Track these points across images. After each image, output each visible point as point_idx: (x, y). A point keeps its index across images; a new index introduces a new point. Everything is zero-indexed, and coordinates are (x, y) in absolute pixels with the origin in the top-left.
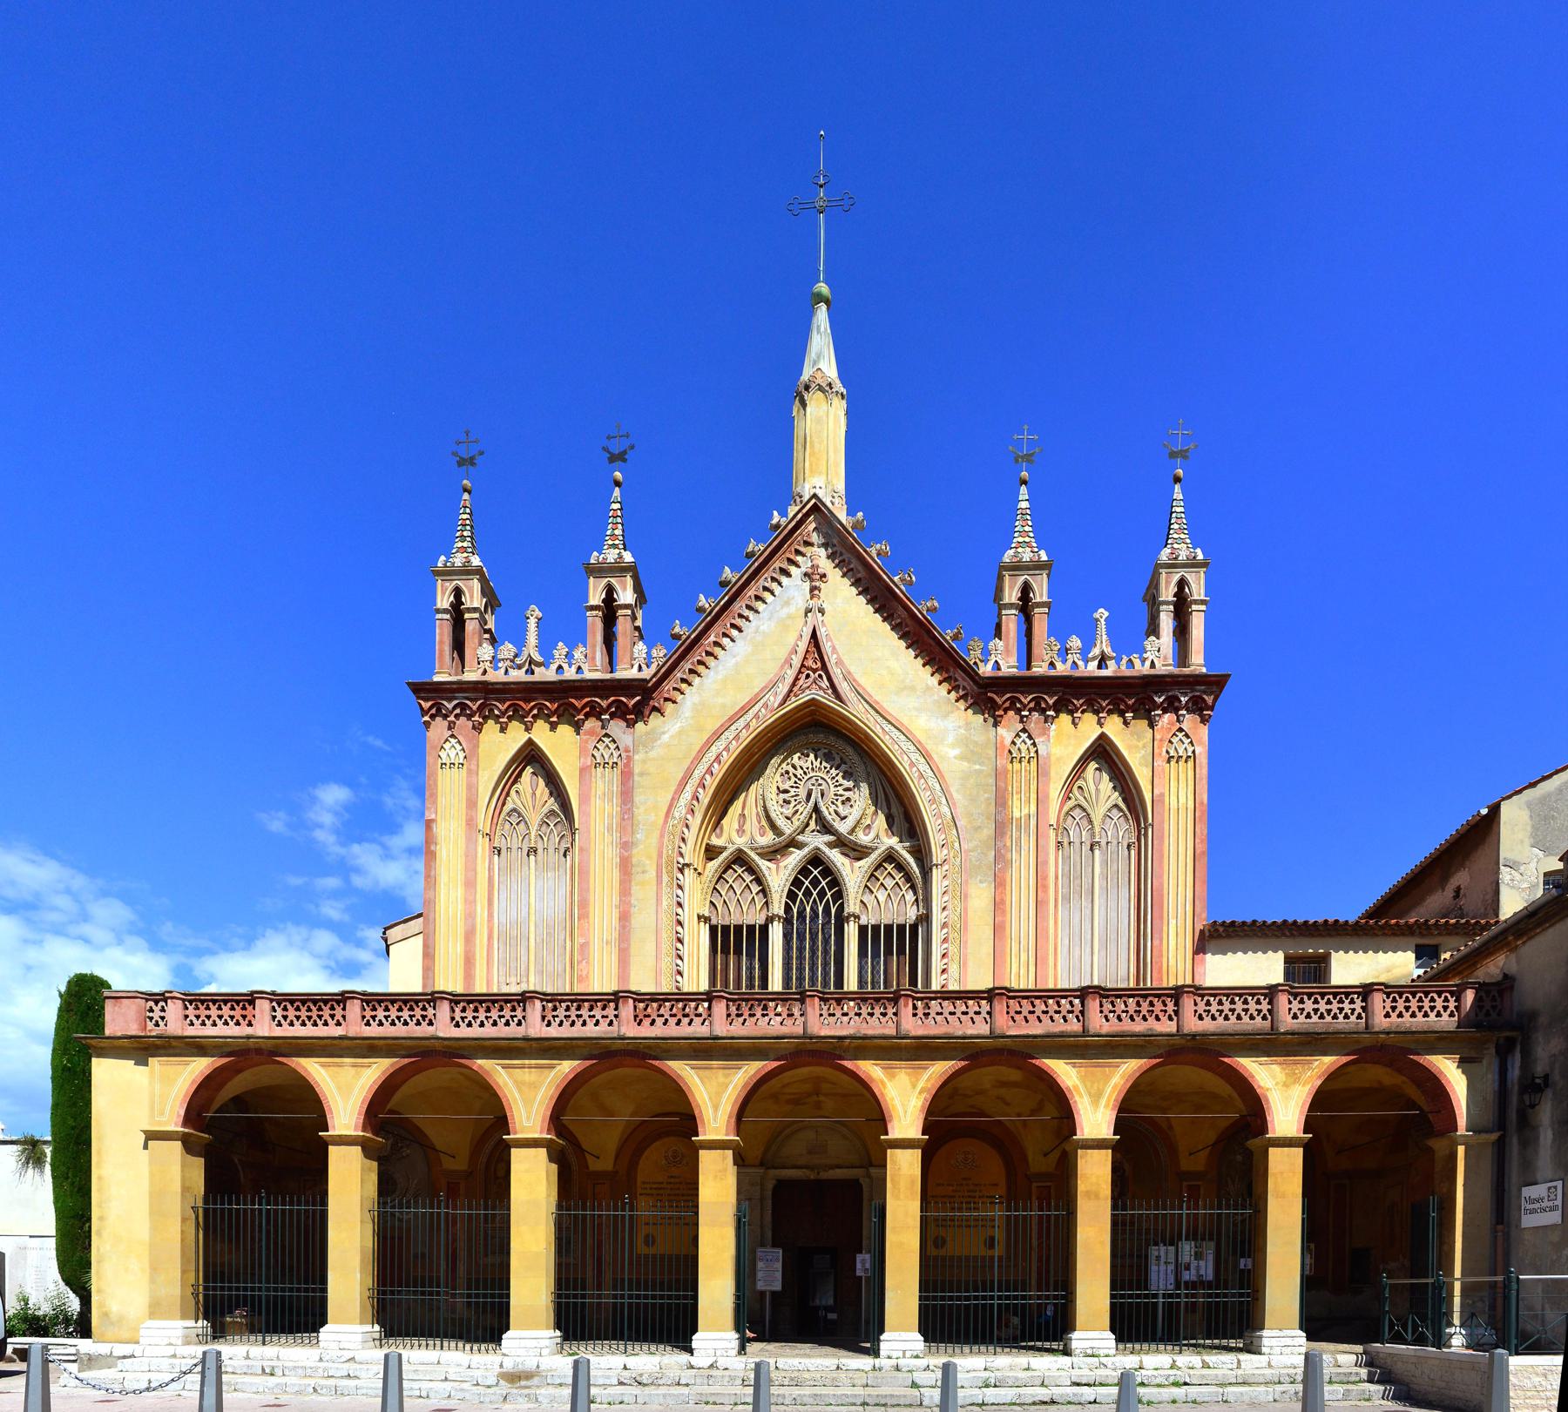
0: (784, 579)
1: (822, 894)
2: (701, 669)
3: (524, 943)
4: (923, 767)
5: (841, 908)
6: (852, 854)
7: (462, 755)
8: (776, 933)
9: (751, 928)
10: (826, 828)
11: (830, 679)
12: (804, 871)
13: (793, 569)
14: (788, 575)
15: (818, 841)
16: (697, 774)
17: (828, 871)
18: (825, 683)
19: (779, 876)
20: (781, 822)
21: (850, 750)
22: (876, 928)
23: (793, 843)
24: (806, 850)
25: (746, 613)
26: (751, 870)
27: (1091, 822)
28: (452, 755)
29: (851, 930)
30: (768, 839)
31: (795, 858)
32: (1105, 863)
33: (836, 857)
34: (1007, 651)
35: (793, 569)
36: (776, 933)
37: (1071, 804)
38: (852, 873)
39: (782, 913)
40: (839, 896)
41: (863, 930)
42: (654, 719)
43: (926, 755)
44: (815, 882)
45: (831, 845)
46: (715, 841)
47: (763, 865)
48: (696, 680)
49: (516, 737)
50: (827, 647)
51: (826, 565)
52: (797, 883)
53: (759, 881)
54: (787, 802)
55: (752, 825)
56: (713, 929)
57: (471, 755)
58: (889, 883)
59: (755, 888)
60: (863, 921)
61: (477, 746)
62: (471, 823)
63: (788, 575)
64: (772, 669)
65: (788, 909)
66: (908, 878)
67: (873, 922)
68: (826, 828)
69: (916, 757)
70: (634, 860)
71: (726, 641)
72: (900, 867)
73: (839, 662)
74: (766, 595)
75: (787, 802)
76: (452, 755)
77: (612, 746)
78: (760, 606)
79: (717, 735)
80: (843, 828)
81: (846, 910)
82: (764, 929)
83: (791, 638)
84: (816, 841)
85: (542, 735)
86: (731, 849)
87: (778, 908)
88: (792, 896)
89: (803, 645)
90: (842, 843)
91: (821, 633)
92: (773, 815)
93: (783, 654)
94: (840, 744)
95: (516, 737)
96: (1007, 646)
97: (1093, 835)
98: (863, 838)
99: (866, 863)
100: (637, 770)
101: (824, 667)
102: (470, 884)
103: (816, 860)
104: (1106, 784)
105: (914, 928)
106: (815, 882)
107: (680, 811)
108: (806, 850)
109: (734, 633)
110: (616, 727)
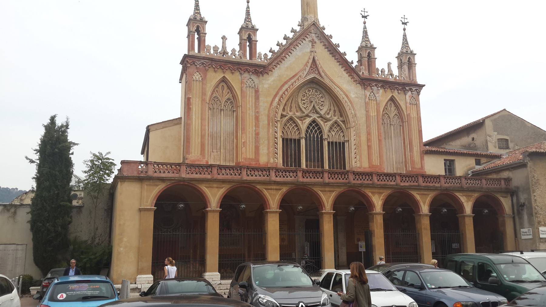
0: (304, 41)
1: (316, 131)
2: (280, 63)
3: (219, 139)
4: (346, 99)
5: (322, 136)
6: (325, 120)
7: (201, 78)
8: (303, 142)
9: (295, 140)
10: (317, 112)
11: (318, 71)
12: (310, 124)
13: (306, 39)
14: (305, 40)
15: (315, 116)
16: (281, 93)
17: (317, 125)
18: (317, 72)
19: (304, 125)
20: (303, 109)
21: (323, 91)
22: (332, 143)
23: (307, 116)
24: (311, 118)
25: (293, 49)
26: (294, 122)
27: (390, 118)
28: (197, 78)
29: (325, 143)
30: (299, 114)
31: (308, 121)
32: (394, 130)
33: (319, 120)
34: (365, 69)
35: (306, 39)
36: (303, 142)
37: (385, 112)
38: (325, 127)
39: (304, 136)
40: (321, 132)
41: (329, 143)
42: (265, 75)
43: (347, 96)
44: (314, 128)
45: (318, 117)
46: (284, 113)
47: (299, 122)
48: (278, 66)
49: (219, 76)
50: (318, 62)
51: (316, 40)
52: (308, 128)
53: (297, 126)
54: (304, 103)
55: (294, 109)
56: (283, 139)
57: (204, 79)
58: (336, 130)
59: (296, 128)
60: (329, 140)
61: (206, 76)
62: (203, 100)
63: (305, 40)
64: (301, 66)
65: (306, 135)
66: (341, 129)
67: (331, 141)
68: (317, 112)
69: (344, 96)
70: (260, 117)
71: (287, 56)
72: (338, 125)
73: (321, 67)
74: (299, 45)
75: (304, 103)
76: (197, 78)
77: (252, 82)
78: (297, 48)
79: (286, 83)
80: (322, 113)
81: (324, 137)
82: (299, 141)
83: (306, 58)
84: (315, 116)
85: (229, 76)
86: (289, 116)
87: (303, 135)
88: (307, 131)
89: (311, 61)
90: (321, 117)
91: (316, 58)
92: (301, 107)
93: (305, 62)
94: (321, 89)
95: (219, 76)
96: (365, 68)
97: (390, 122)
98: (328, 117)
99: (329, 123)
100: (260, 90)
101: (317, 67)
102: (202, 119)
103: (314, 121)
104: (393, 108)
105: (343, 143)
106: (314, 128)
107: (275, 104)
108: (311, 118)
109: (290, 54)
110: (254, 77)
